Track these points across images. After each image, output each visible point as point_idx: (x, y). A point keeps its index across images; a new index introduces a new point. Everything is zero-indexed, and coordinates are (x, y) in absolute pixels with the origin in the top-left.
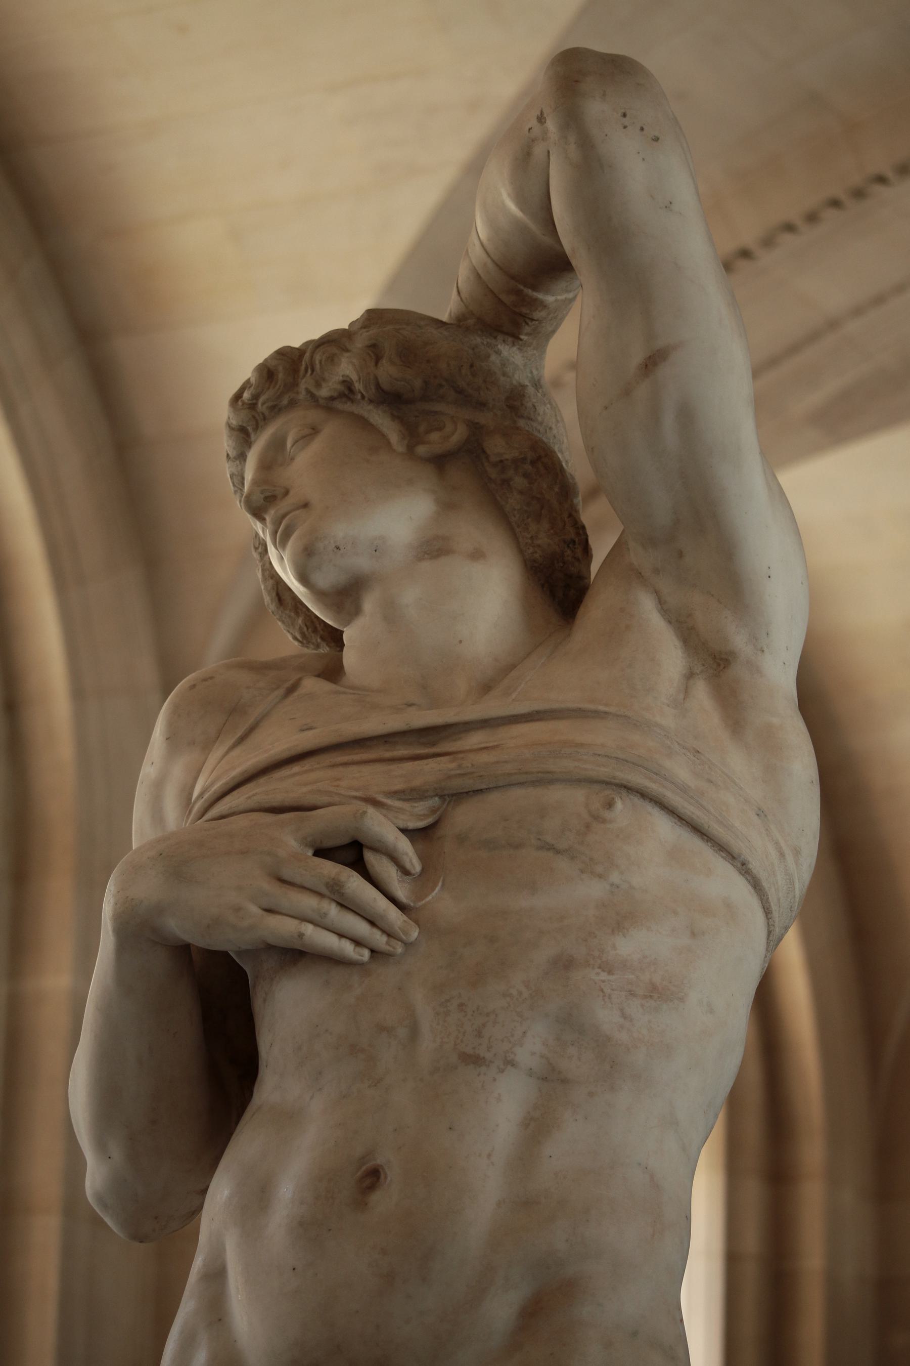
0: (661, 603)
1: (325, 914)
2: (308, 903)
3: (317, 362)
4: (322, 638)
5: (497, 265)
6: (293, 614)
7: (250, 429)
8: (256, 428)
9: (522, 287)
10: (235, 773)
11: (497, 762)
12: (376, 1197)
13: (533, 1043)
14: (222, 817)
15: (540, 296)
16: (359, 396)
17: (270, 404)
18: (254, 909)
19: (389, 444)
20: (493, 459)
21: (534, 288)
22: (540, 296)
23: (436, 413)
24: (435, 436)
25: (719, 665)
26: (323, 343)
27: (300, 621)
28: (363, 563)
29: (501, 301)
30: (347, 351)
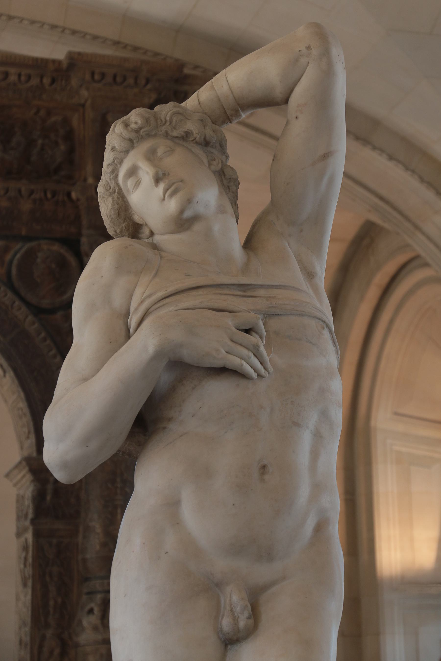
0: (291, 248)
1: (250, 358)
2: (245, 352)
3: (174, 121)
4: (129, 234)
5: (235, 98)
6: (122, 221)
7: (135, 141)
8: (138, 142)
9: (239, 109)
10: (171, 289)
11: (284, 304)
12: (266, 477)
13: (312, 419)
14: (188, 309)
15: (242, 114)
16: (191, 139)
17: (147, 133)
18: (223, 351)
19: (203, 162)
20: (228, 177)
21: (243, 110)
22: (242, 114)
23: (212, 153)
24: (214, 163)
25: (310, 277)
26: (176, 113)
27: (124, 225)
29: (225, 112)
30: (189, 120)
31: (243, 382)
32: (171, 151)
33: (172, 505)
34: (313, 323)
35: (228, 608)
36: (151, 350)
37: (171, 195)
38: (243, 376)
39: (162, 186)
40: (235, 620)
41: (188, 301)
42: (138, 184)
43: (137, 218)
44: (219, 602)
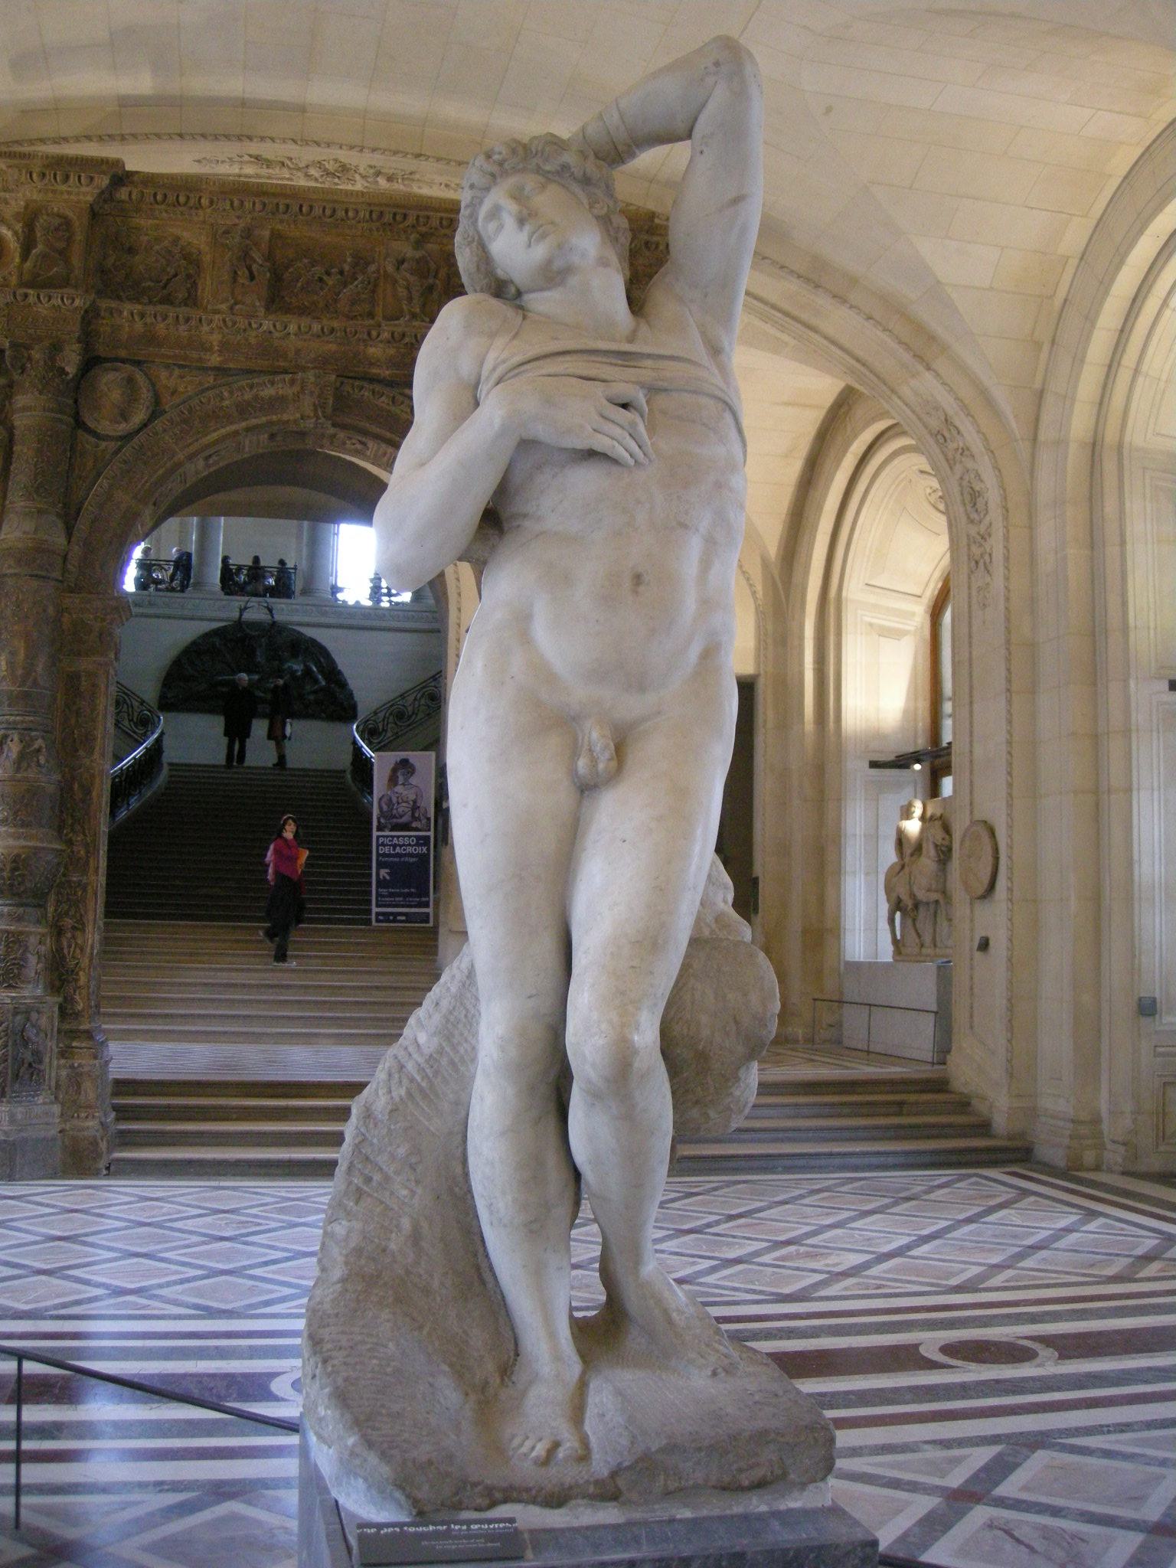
10: (530, 354)
12: (641, 588)
13: (704, 521)
28: (576, 259)
31: (615, 469)
32: (543, 187)
33: (521, 622)
34: (711, 403)
35: (586, 747)
36: (497, 422)
37: (538, 241)
38: (616, 461)
39: (527, 228)
40: (594, 761)
41: (550, 367)
42: (501, 227)
43: (500, 273)
44: (575, 740)
